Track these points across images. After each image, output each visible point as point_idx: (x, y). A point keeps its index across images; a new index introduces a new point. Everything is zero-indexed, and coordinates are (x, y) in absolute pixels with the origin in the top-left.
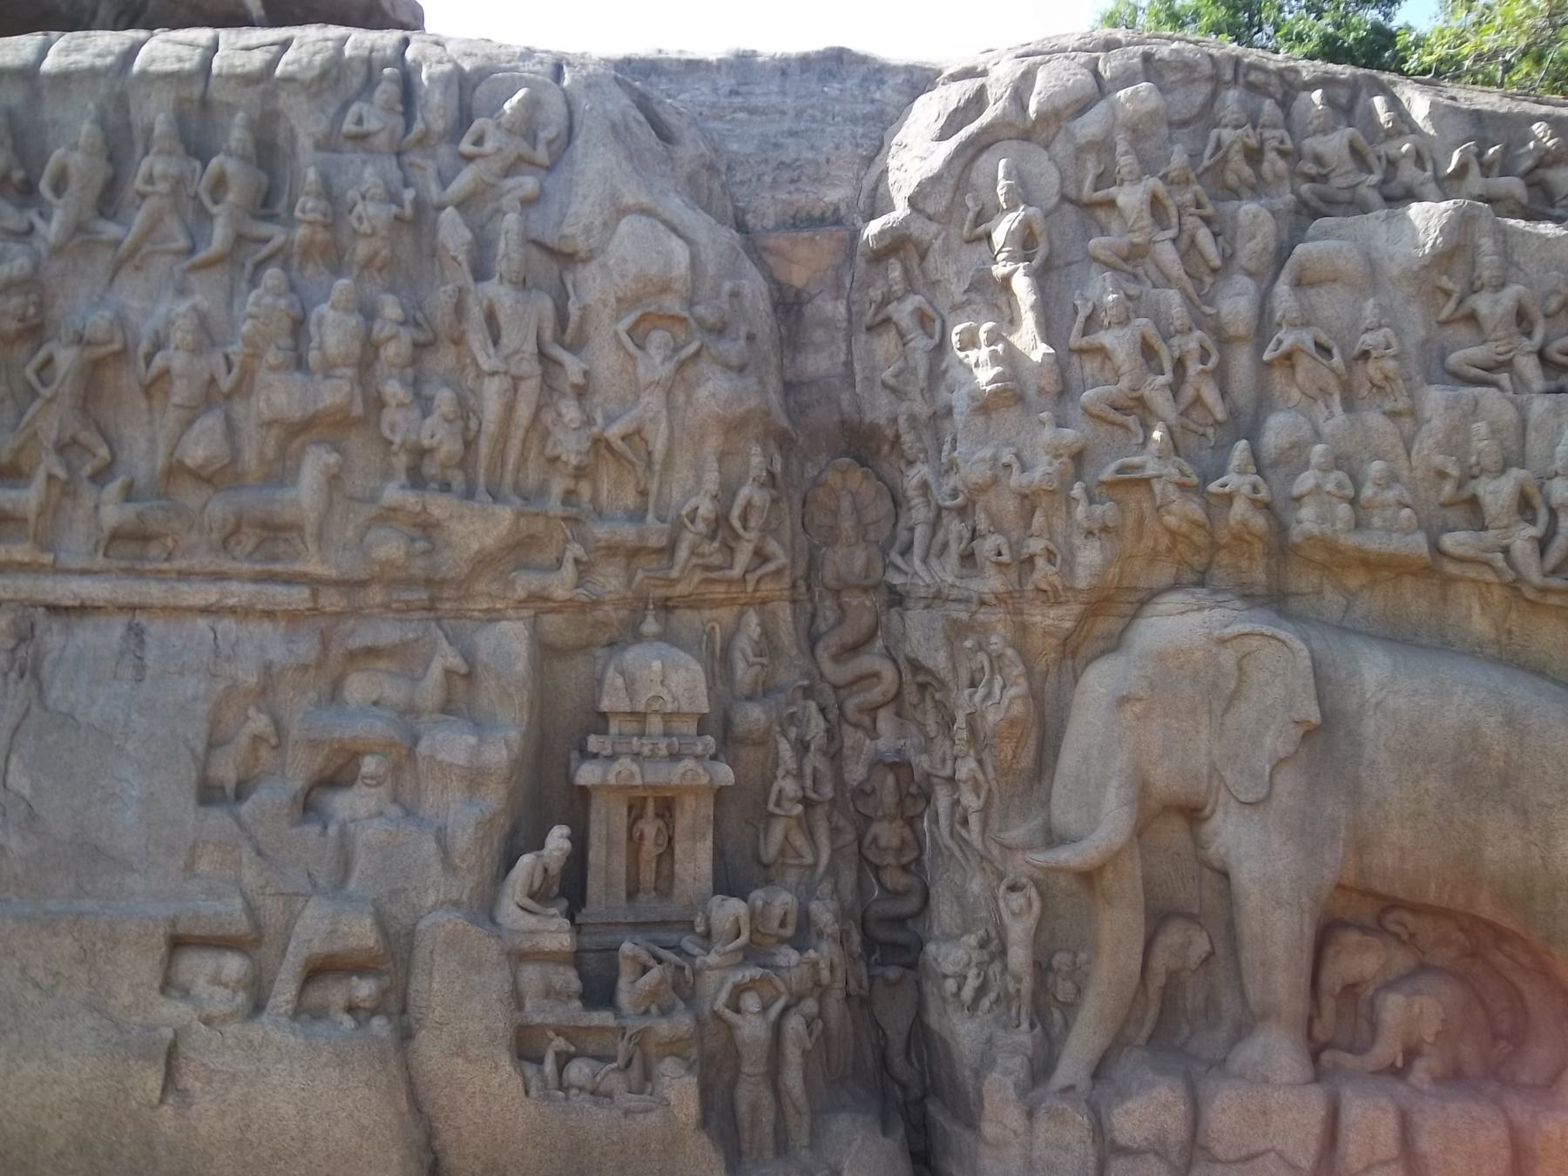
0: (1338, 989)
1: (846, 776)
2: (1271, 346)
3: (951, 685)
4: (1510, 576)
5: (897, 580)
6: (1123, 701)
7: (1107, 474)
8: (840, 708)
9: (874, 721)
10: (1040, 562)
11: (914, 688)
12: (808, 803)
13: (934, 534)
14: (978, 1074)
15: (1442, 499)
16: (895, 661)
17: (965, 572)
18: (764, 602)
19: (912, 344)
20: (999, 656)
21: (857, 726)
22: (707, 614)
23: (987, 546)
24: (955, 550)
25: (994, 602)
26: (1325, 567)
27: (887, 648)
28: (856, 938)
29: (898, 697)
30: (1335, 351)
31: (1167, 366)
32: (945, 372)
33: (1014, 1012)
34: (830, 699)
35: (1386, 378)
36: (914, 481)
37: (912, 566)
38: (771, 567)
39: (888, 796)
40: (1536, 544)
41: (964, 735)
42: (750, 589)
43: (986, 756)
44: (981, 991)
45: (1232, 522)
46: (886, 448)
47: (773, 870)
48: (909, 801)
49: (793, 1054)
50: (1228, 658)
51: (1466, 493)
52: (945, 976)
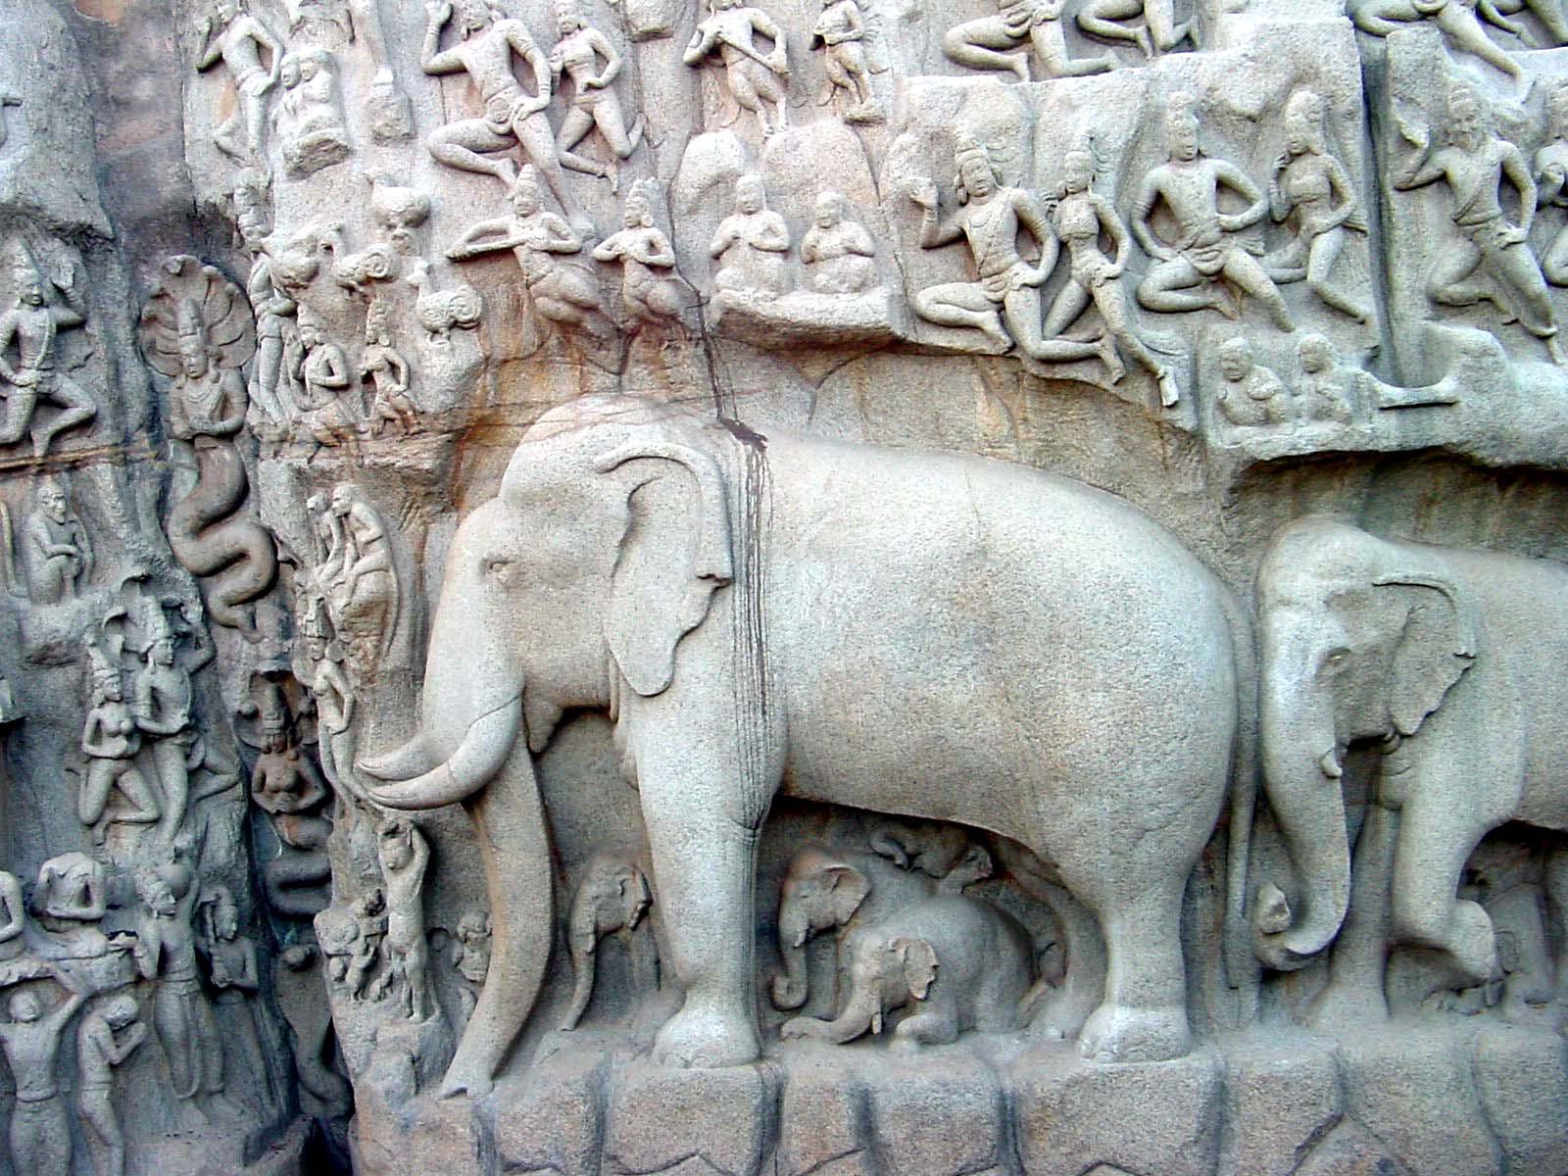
0: (801, 937)
1: (224, 694)
2: (694, 41)
3: (308, 561)
4: (1006, 341)
5: (253, 418)
6: (489, 565)
7: (460, 246)
8: (204, 602)
10: (382, 380)
12: (145, 741)
14: (357, 1076)
15: (922, 239)
17: (307, 401)
18: (74, 466)
19: (244, 87)
20: (346, 515)
21: (230, 626)
23: (312, 367)
24: (292, 367)
25: (332, 441)
26: (773, 352)
28: (227, 913)
29: (273, 584)
30: (778, 40)
31: (543, 77)
32: (275, 124)
33: (404, 996)
34: (184, 591)
35: (849, 72)
38: (70, 417)
39: (270, 722)
40: (1033, 296)
41: (314, 629)
42: (39, 451)
43: (345, 656)
44: (370, 971)
45: (627, 298)
47: (99, 831)
48: (304, 724)
49: (94, 1071)
50: (614, 492)
51: (949, 228)
52: (330, 956)
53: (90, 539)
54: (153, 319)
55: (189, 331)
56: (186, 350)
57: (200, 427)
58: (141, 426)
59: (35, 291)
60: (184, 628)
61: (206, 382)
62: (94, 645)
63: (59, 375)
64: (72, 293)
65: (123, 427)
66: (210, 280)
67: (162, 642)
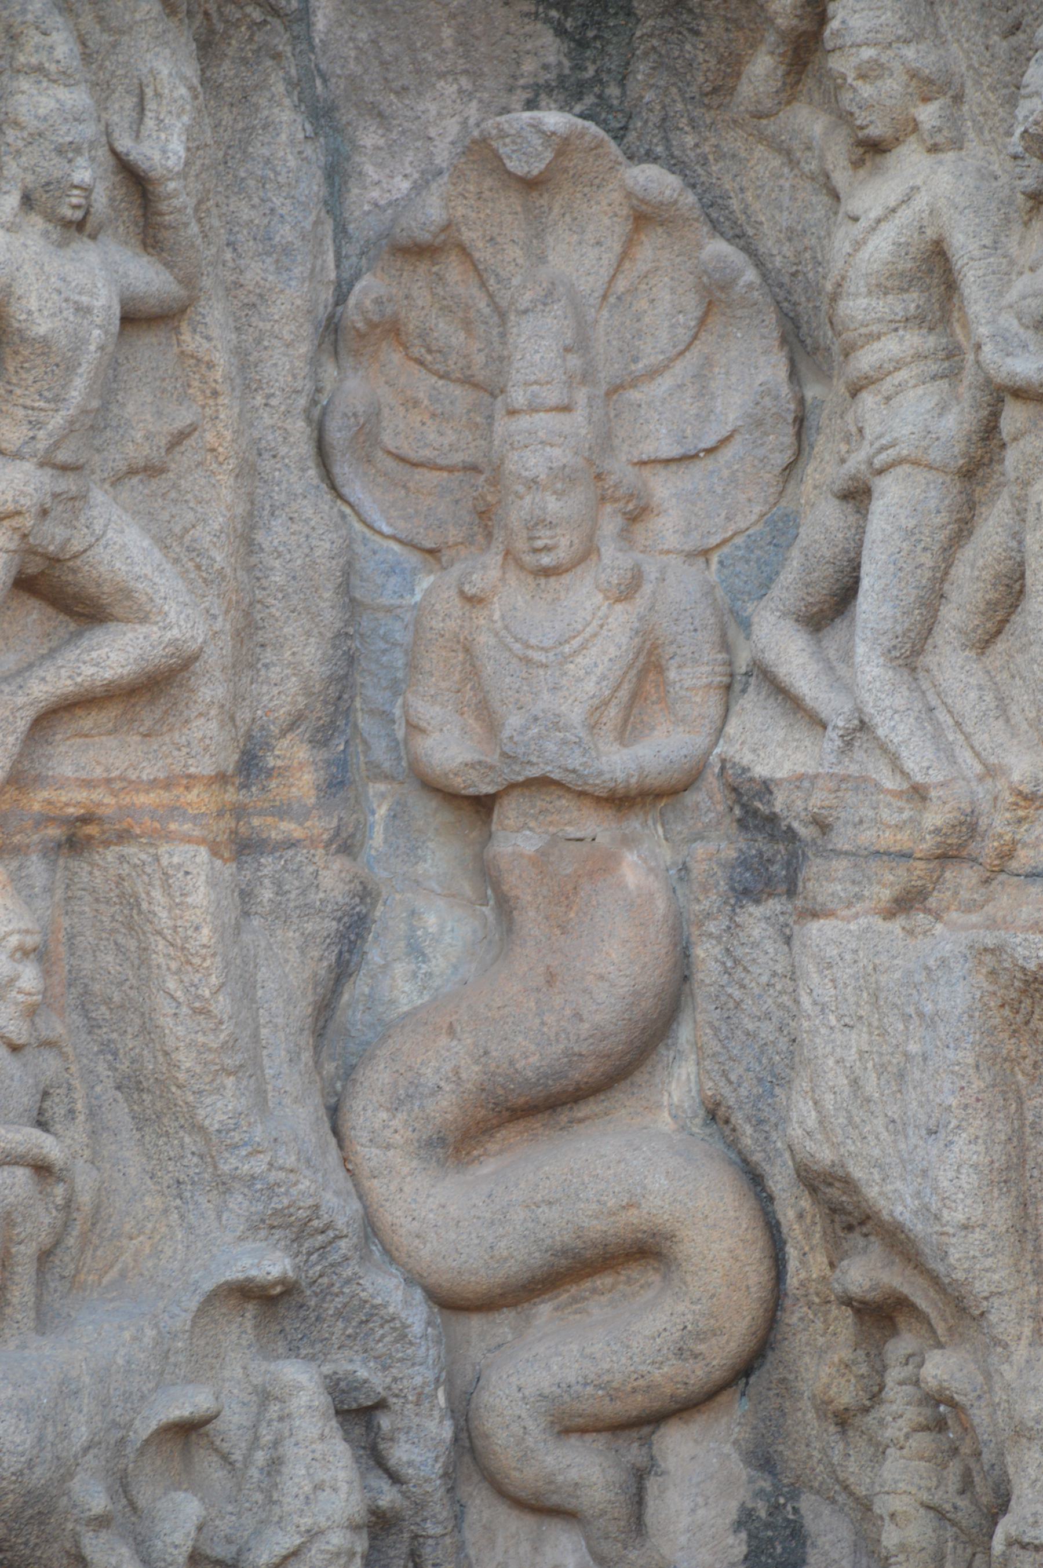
9: (638, 1482)
11: (844, 1322)
13: (963, 528)
16: (755, 1179)
21: (545, 1508)
27: (714, 1114)
36: (880, 248)
37: (838, 671)
38: (111, 655)
46: (762, 68)
53: (92, 1115)
54: (391, 329)
55: (553, 396)
56: (533, 462)
57: (552, 758)
59: (83, 174)
60: (388, 1497)
61: (583, 598)
62: (102, 1522)
63: (98, 496)
64: (178, 196)
65: (244, 715)
66: (644, 217)
67: (337, 1539)
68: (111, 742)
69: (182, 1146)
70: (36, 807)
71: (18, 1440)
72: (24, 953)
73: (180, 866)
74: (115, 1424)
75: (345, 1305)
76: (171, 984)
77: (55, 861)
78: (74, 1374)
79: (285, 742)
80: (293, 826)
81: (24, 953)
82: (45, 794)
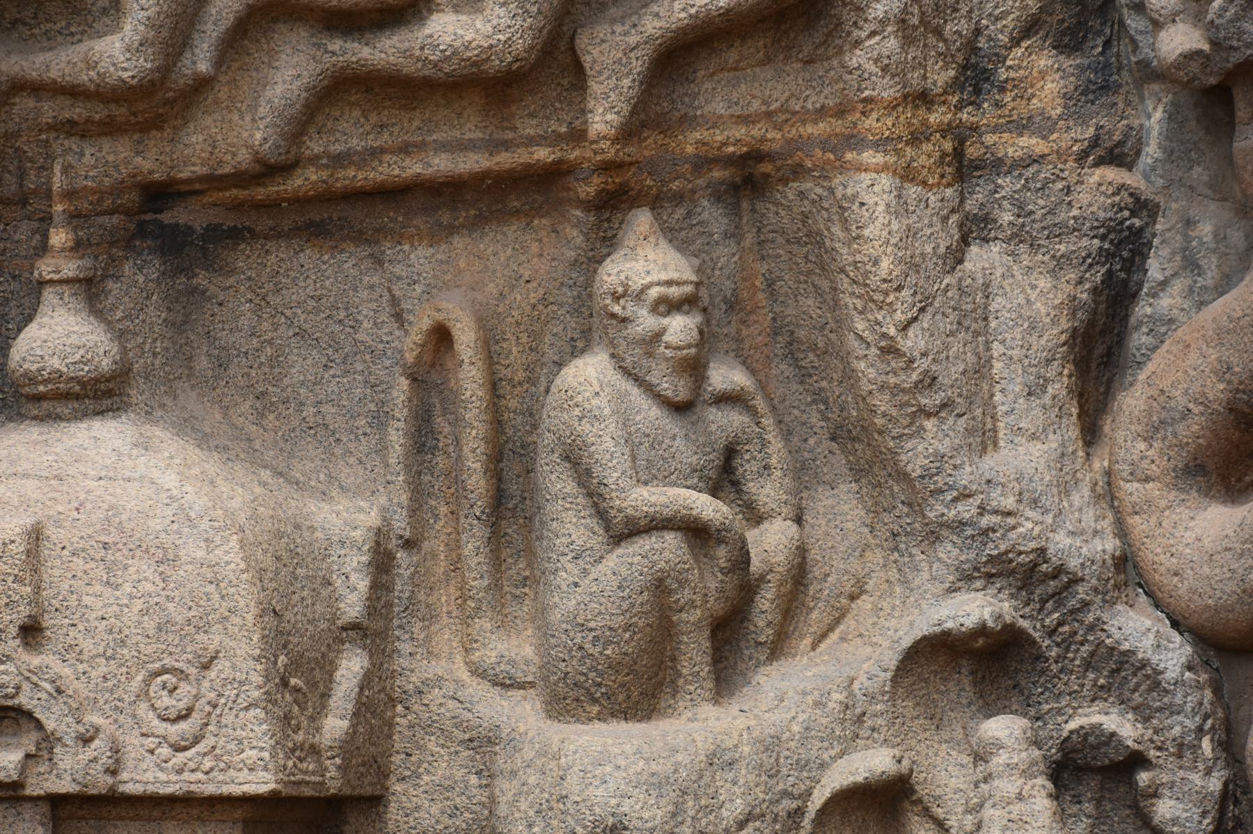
22: (419, 259)
42: (603, 118)
58: (1029, 28)
65: (957, 26)
68: (768, 72)
69: (892, 495)
70: (690, 149)
71: (646, 815)
72: (667, 306)
73: (855, 196)
74: (785, 794)
75: (1092, 654)
76: (860, 325)
77: (736, 206)
78: (729, 743)
79: (1018, 52)
80: (1034, 141)
81: (667, 306)
82: (697, 135)
